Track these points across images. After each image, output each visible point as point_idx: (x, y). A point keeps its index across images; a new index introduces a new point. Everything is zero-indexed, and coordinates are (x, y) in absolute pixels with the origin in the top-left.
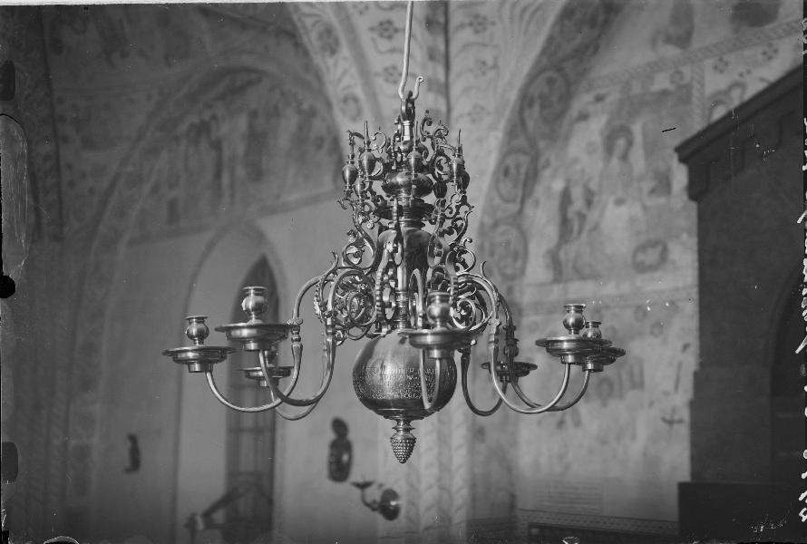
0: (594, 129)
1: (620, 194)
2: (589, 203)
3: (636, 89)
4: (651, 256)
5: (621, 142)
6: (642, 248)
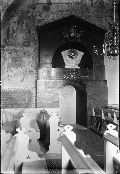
0: (16, 19)
1: (21, 32)
2: (14, 32)
3: (25, 14)
4: (27, 44)
5: (21, 23)
6: (25, 42)
